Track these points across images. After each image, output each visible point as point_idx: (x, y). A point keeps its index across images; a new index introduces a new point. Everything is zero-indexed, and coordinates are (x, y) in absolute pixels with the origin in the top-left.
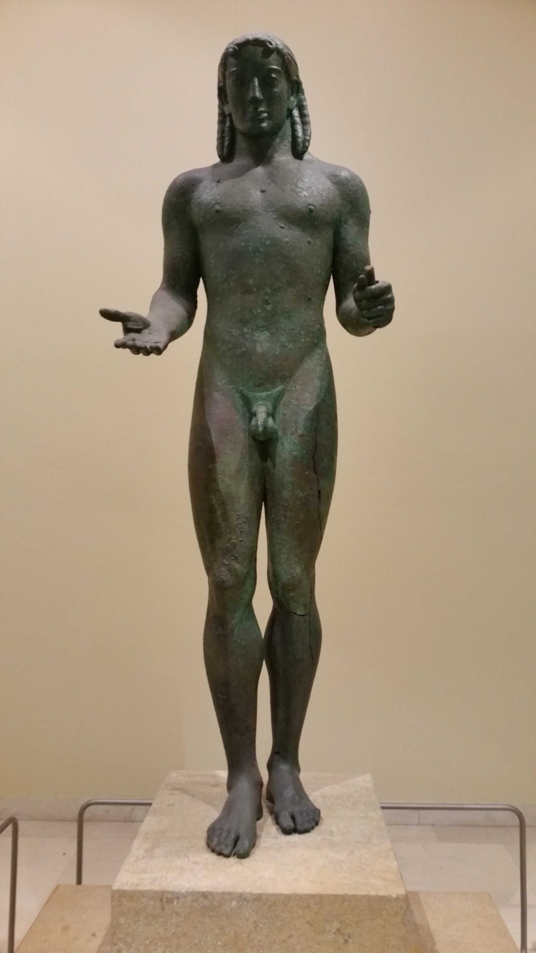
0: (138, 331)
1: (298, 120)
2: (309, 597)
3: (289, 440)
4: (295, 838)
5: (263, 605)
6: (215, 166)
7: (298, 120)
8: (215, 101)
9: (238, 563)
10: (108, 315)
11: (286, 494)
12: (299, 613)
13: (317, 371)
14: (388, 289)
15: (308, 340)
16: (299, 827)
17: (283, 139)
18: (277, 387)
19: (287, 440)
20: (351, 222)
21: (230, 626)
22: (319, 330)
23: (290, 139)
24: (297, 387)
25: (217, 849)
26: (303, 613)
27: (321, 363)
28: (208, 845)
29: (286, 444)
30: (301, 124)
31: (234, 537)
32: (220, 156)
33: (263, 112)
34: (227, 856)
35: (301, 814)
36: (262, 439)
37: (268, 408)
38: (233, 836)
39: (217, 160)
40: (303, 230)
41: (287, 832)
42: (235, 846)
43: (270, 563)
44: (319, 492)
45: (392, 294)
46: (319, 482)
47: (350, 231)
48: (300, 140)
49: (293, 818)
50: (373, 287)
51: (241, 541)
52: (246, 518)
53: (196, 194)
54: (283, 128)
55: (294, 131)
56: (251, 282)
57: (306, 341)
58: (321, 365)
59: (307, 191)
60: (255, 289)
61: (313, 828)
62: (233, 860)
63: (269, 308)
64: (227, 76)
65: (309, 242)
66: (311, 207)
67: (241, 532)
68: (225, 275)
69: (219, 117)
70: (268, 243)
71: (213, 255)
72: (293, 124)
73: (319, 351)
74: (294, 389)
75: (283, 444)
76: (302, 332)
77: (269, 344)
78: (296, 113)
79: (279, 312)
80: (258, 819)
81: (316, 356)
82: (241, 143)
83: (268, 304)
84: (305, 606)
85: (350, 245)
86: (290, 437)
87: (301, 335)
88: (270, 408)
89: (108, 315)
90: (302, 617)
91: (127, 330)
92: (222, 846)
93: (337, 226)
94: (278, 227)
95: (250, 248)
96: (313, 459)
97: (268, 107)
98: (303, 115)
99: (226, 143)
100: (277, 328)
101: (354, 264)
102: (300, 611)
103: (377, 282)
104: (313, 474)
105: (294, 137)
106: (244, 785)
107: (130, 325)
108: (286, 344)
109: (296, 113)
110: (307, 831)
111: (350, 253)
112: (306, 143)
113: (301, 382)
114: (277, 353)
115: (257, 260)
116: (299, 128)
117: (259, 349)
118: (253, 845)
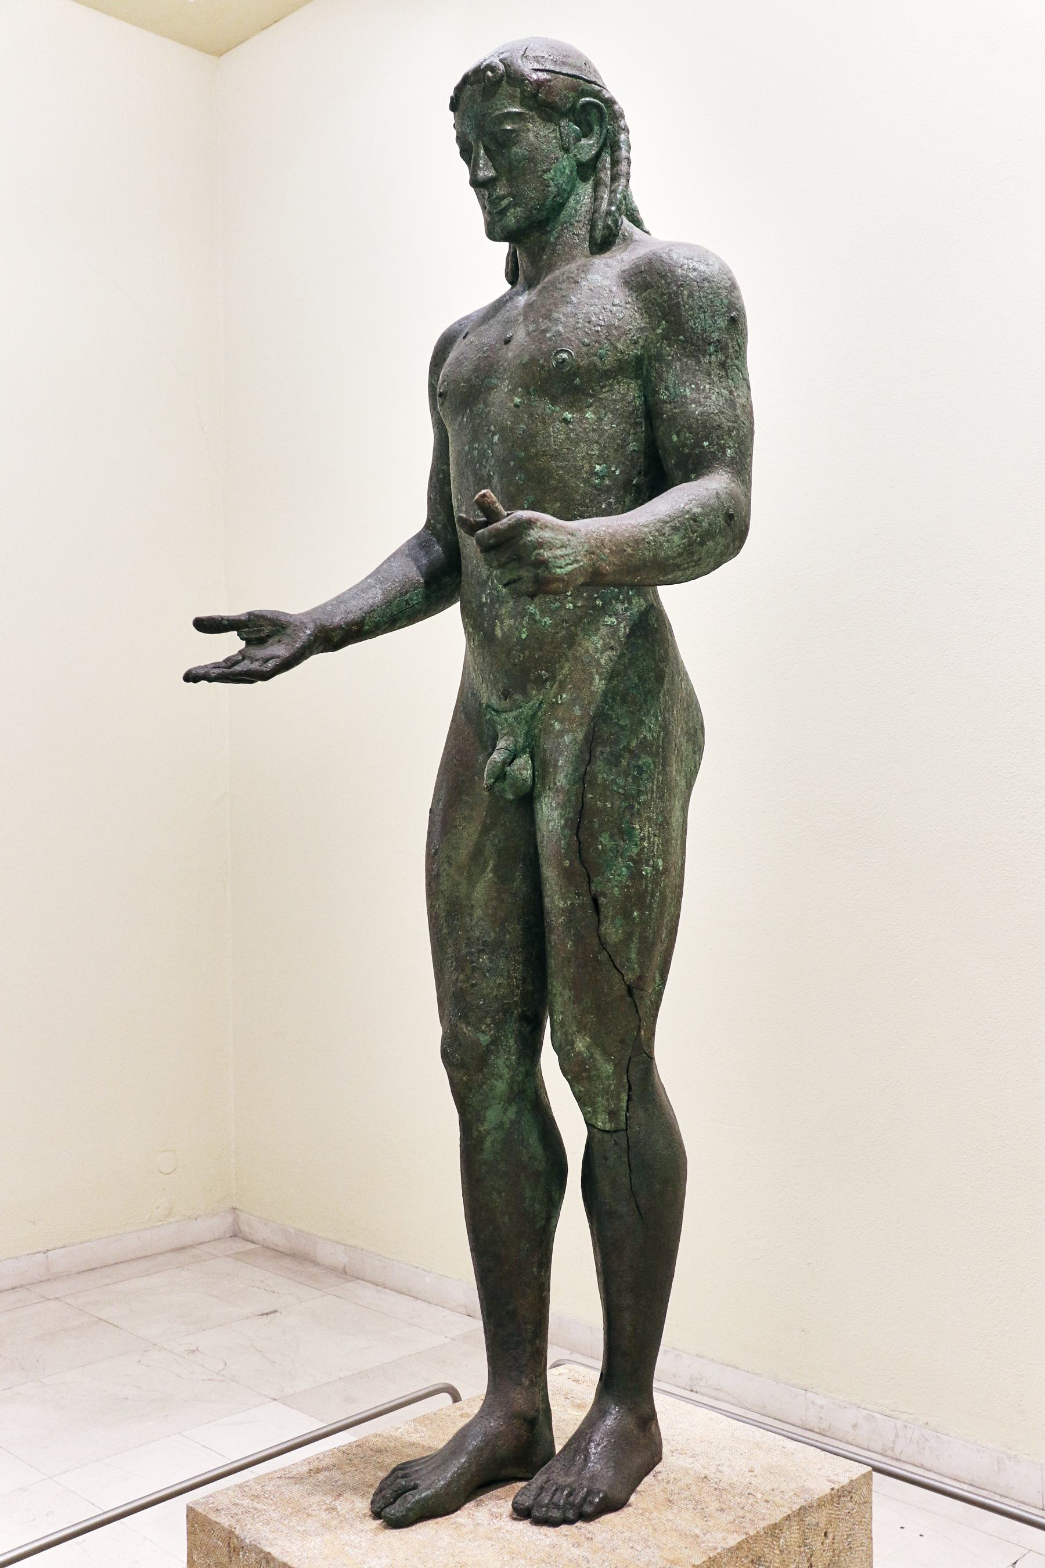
9: (468, 1024)
13: (603, 661)
24: (564, 696)
26: (608, 1127)
33: (504, 197)
44: (595, 901)
46: (590, 882)
51: (473, 985)
58: (612, 648)
67: (474, 969)
77: (512, 622)
81: (603, 631)
84: (613, 1115)
85: (665, 402)
90: (607, 1136)
96: (577, 835)
97: (511, 186)
101: (675, 438)
114: (524, 636)
117: (499, 633)
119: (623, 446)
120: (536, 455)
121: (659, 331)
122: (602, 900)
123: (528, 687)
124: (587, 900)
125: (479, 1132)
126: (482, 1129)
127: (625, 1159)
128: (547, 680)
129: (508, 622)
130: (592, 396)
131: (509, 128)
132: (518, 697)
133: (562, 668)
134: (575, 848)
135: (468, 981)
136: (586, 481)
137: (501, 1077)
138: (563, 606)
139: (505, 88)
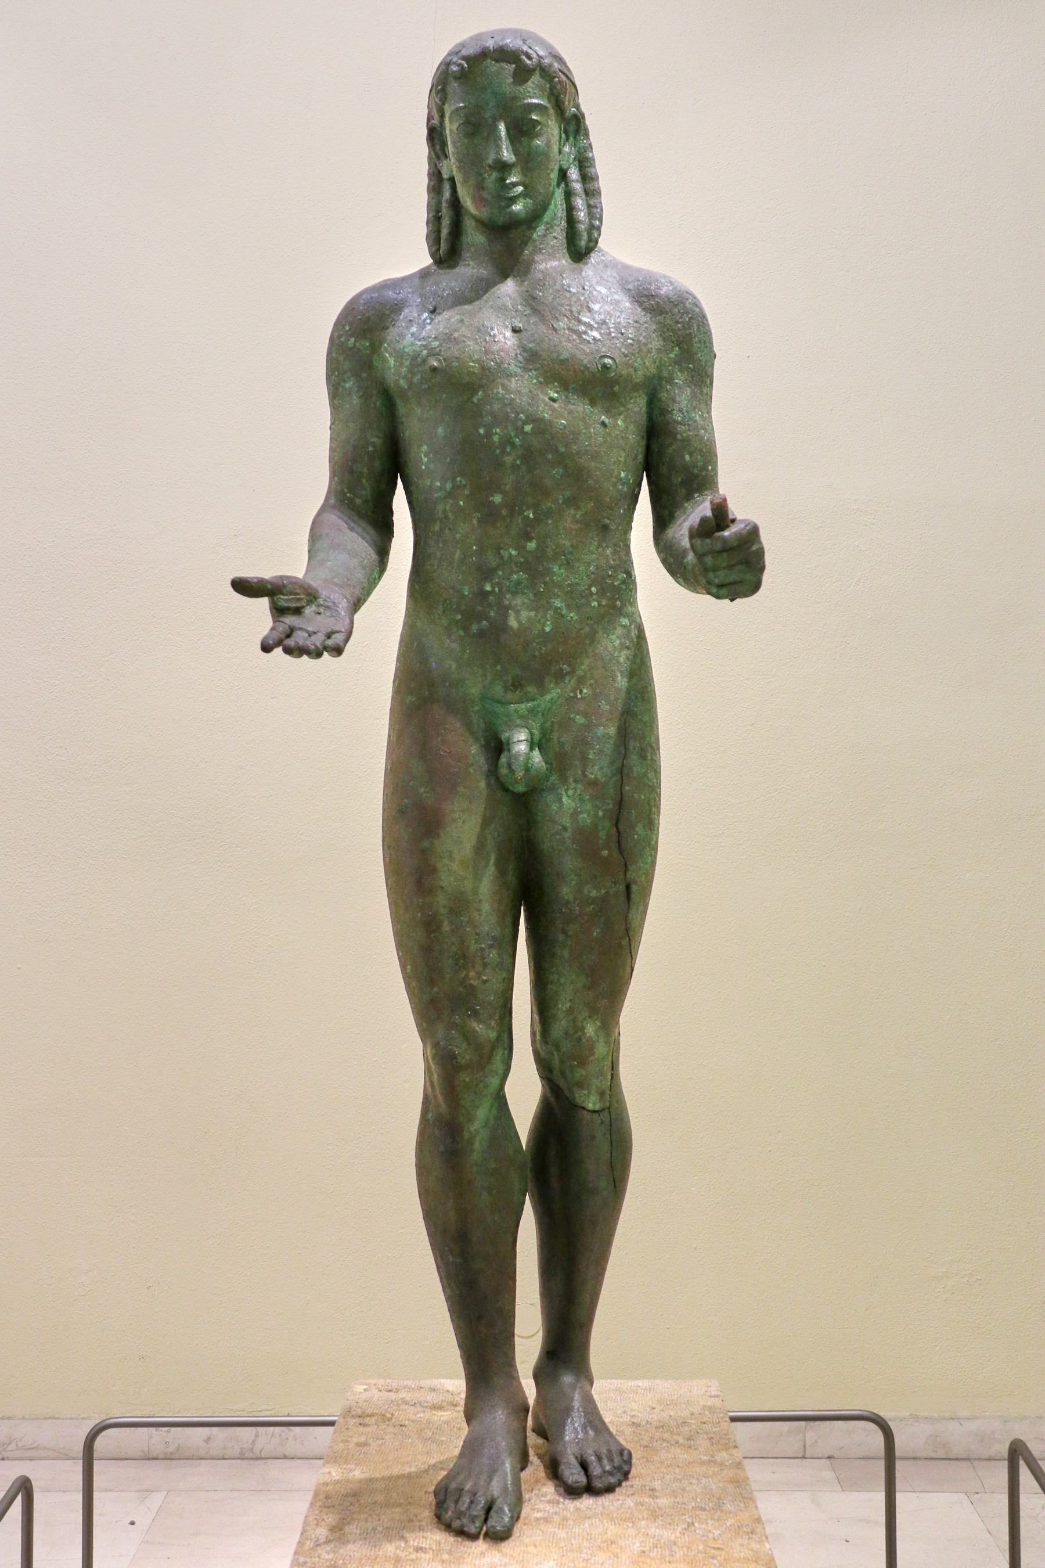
0: (298, 611)
1: (578, 186)
2: (609, 1076)
3: (570, 792)
4: (587, 1502)
5: (524, 1093)
6: (424, 274)
7: (578, 186)
8: (423, 149)
9: (480, 1021)
10: (244, 587)
11: (566, 891)
12: (590, 1106)
13: (621, 660)
14: (753, 534)
15: (604, 603)
16: (598, 1484)
17: (550, 227)
18: (548, 691)
19: (566, 791)
20: (680, 379)
21: (466, 1135)
22: (624, 582)
23: (564, 223)
24: (585, 691)
25: (456, 1524)
26: (597, 1107)
27: (628, 643)
28: (438, 1517)
29: (565, 799)
30: (584, 196)
31: (472, 974)
32: (432, 256)
33: (514, 185)
34: (473, 1537)
35: (599, 1459)
36: (521, 788)
37: (532, 734)
38: (482, 1502)
39: (428, 261)
40: (593, 403)
41: (572, 1492)
42: (486, 1520)
43: (536, 1017)
44: (628, 888)
45: (760, 543)
46: (626, 870)
47: (680, 397)
48: (582, 227)
49: (584, 1466)
50: (726, 533)
51: (485, 982)
52: (494, 938)
53: (392, 334)
54: (552, 207)
55: (570, 209)
56: (497, 499)
57: (599, 605)
58: (628, 648)
59: (597, 329)
60: (504, 512)
61: (620, 1484)
62: (481, 1545)
63: (532, 545)
64: (447, 115)
65: (603, 424)
66: (607, 361)
68: (449, 486)
69: (430, 180)
70: (528, 428)
71: (425, 448)
72: (569, 195)
73: (625, 621)
74: (579, 696)
75: (560, 800)
76: (593, 589)
77: (532, 614)
78: (574, 174)
79: (550, 552)
80: (522, 1469)
81: (619, 631)
82: (474, 237)
83: (530, 539)
84: (602, 1094)
86: (573, 785)
87: (591, 594)
88: (536, 732)
89: (244, 587)
90: (596, 1116)
91: (278, 611)
92: (465, 1521)
93: (654, 393)
94: (547, 399)
95: (496, 438)
97: (525, 175)
98: (586, 177)
99: (445, 232)
100: (545, 583)
101: (687, 457)
102: (592, 1103)
103: (733, 521)
104: (616, 854)
105: (571, 221)
106: (499, 1417)
107: (283, 601)
108: (564, 612)
109: (574, 174)
110: (610, 1489)
111: (679, 437)
112: (594, 230)
113: (592, 681)
114: (548, 629)
115: (508, 459)
116: (579, 202)
117: (513, 623)
118: (516, 1518)
119: (635, 459)
120: (578, 453)
121: (672, 356)
122: (634, 888)
123: (547, 680)
124: (622, 888)
125: (470, 1132)
126: (472, 1129)
127: (608, 1136)
128: (568, 673)
129: (524, 614)
130: (624, 406)
131: (534, 117)
132: (531, 689)
133: (582, 664)
134: (615, 839)
135: (479, 978)
136: (614, 485)
137: (496, 1073)
138: (589, 603)
139: (536, 78)
